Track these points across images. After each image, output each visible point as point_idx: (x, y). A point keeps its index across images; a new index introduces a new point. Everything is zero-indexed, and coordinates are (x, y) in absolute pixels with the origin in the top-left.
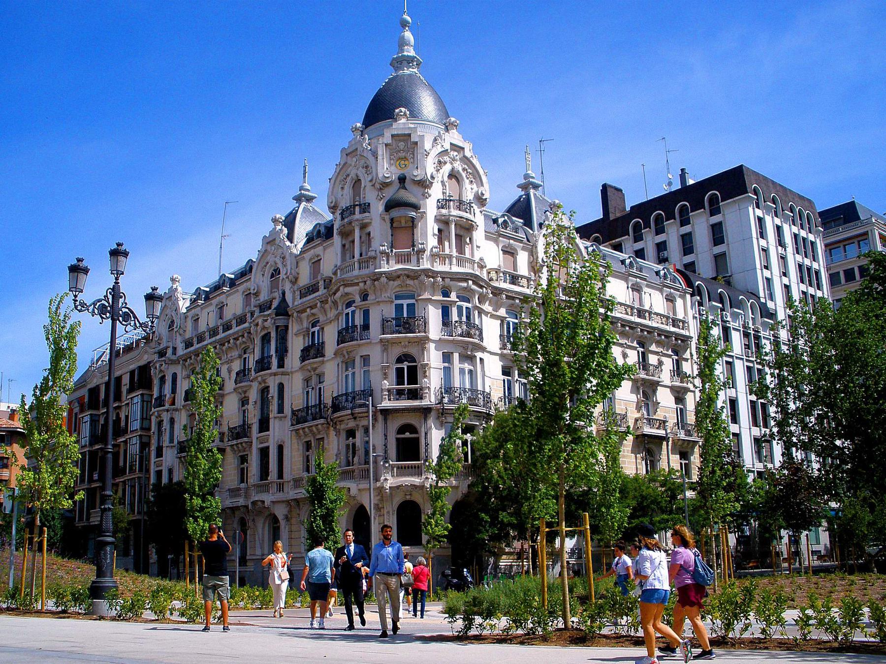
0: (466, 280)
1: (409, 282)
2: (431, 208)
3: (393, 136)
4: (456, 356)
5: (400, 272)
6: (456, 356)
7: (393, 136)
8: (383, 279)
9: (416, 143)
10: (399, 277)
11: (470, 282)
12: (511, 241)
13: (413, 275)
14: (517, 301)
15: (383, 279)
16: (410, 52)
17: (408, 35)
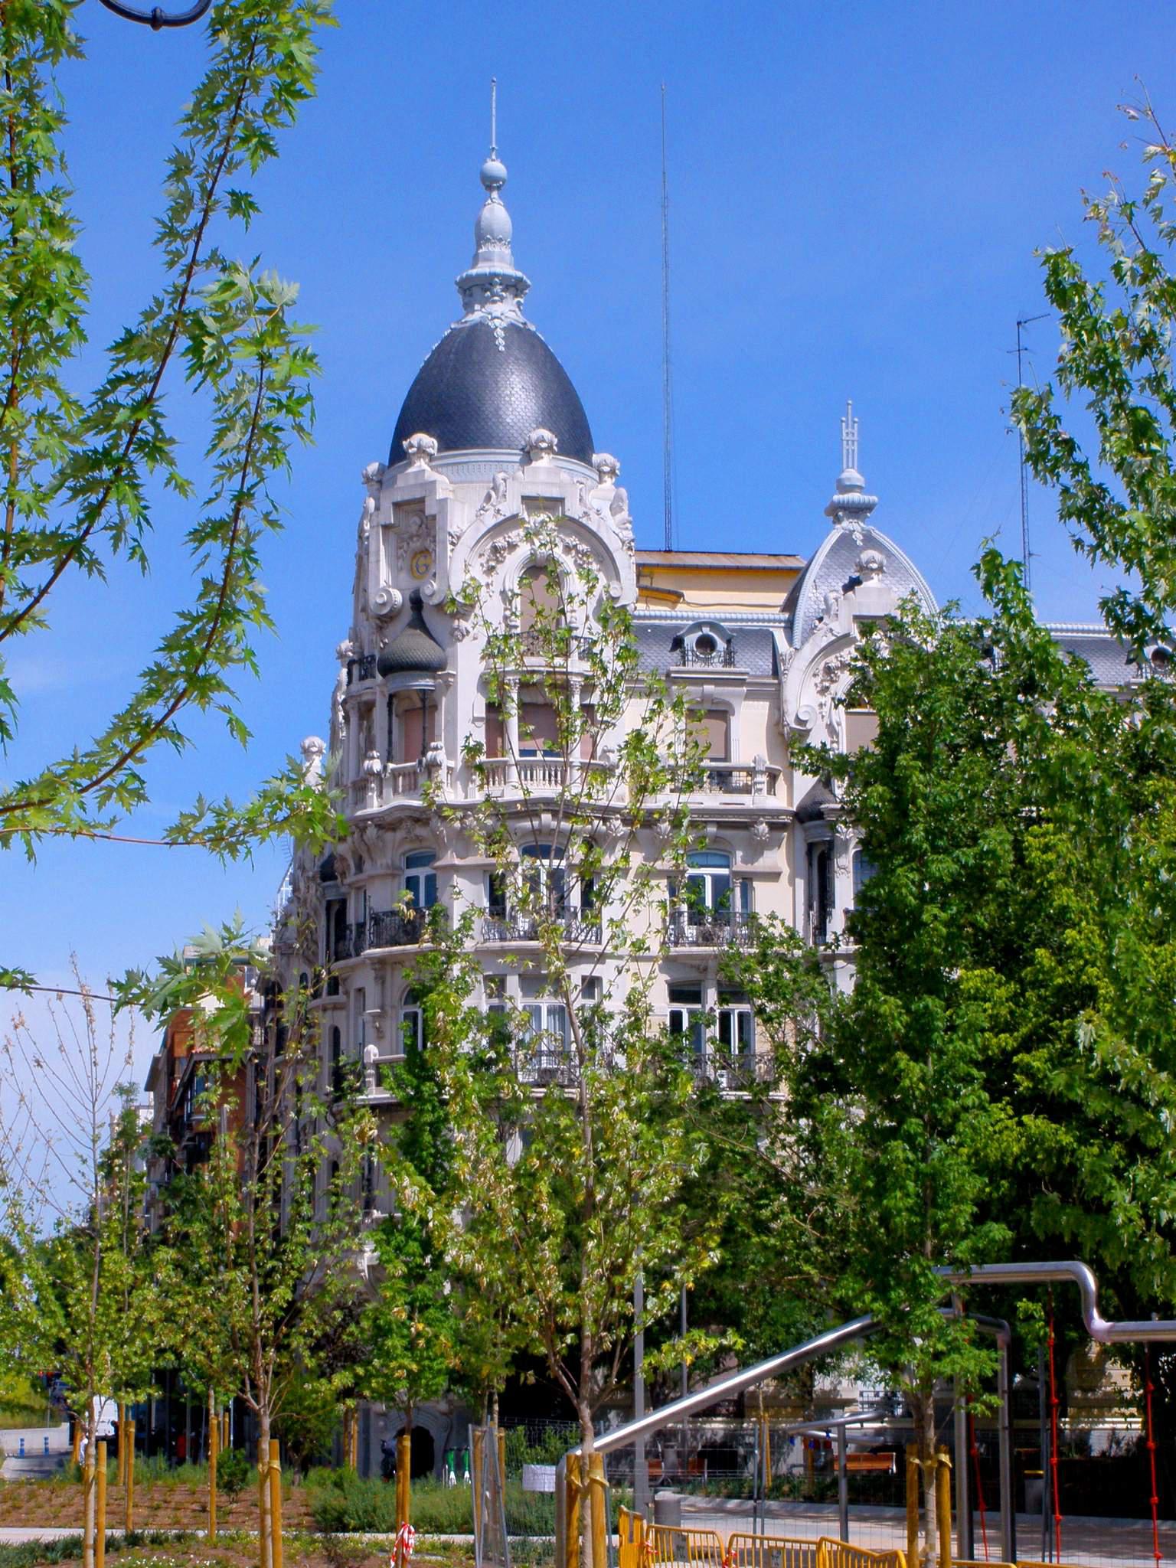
0: (536, 814)
1: (420, 831)
2: (468, 663)
3: (397, 505)
4: (513, 983)
5: (398, 814)
6: (513, 983)
7: (397, 505)
8: (371, 832)
9: (434, 517)
10: (401, 821)
11: (546, 817)
12: (709, 688)
13: (419, 818)
14: (712, 829)
15: (371, 832)
16: (499, 261)
17: (496, 213)
